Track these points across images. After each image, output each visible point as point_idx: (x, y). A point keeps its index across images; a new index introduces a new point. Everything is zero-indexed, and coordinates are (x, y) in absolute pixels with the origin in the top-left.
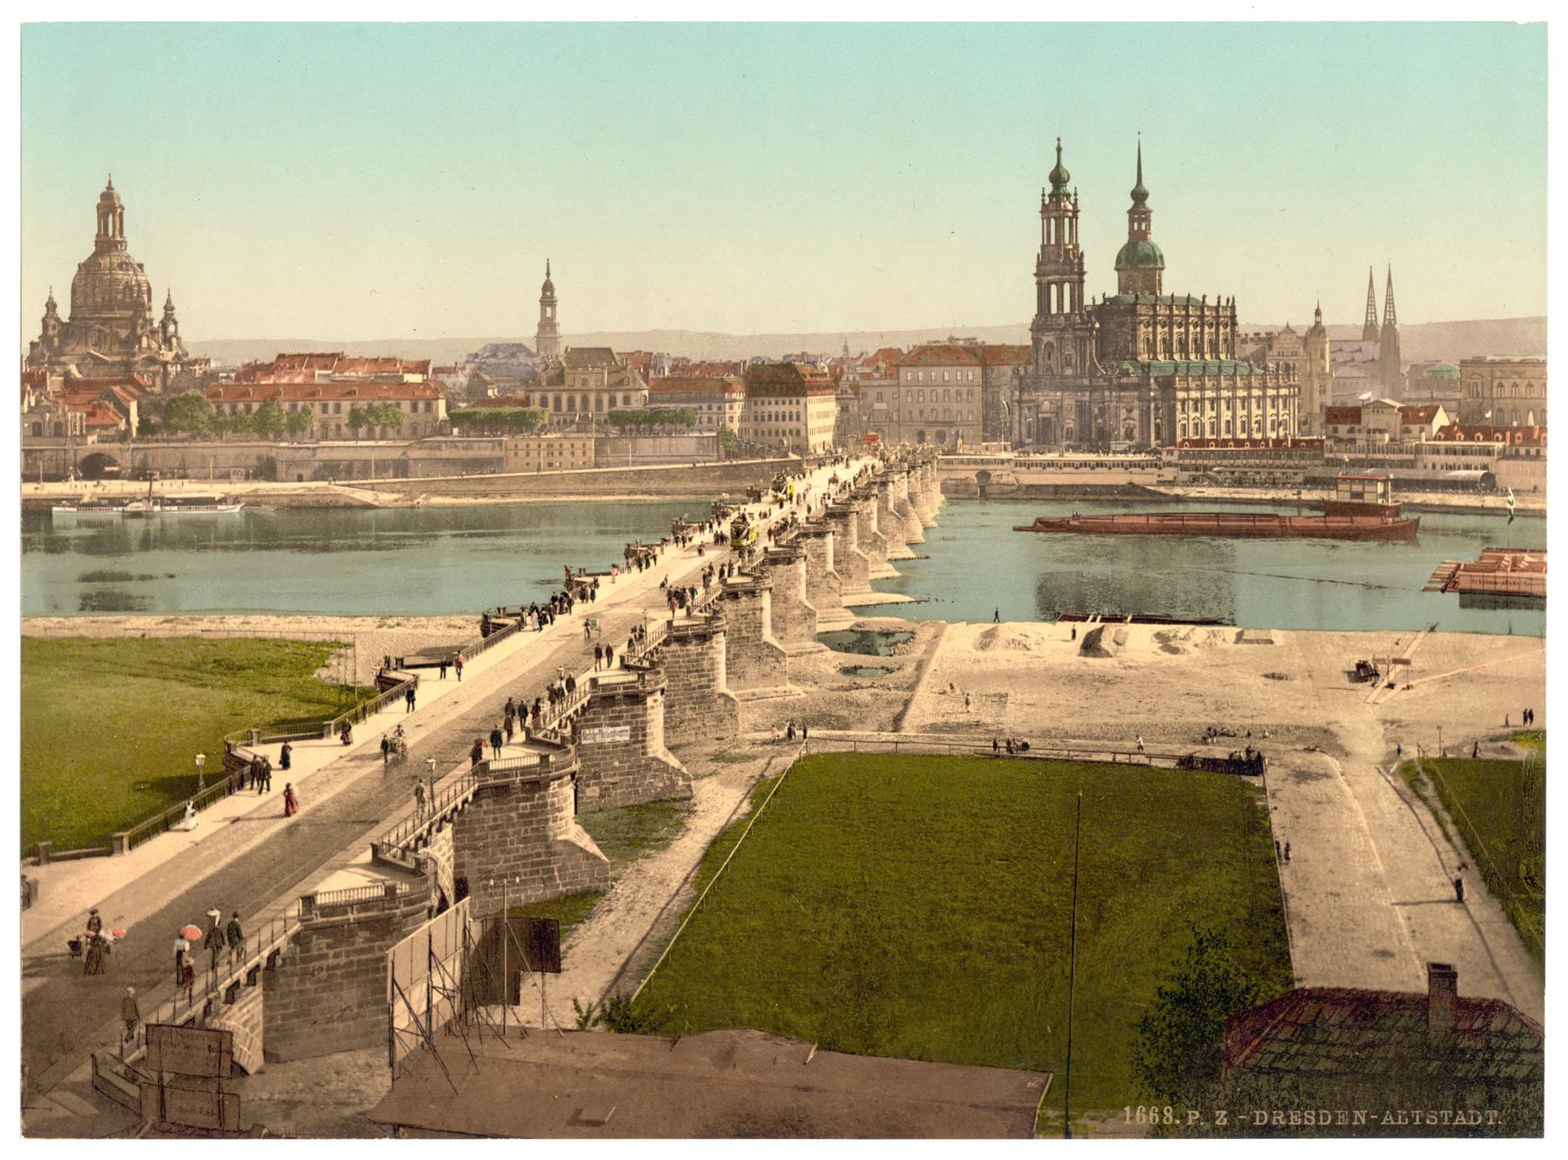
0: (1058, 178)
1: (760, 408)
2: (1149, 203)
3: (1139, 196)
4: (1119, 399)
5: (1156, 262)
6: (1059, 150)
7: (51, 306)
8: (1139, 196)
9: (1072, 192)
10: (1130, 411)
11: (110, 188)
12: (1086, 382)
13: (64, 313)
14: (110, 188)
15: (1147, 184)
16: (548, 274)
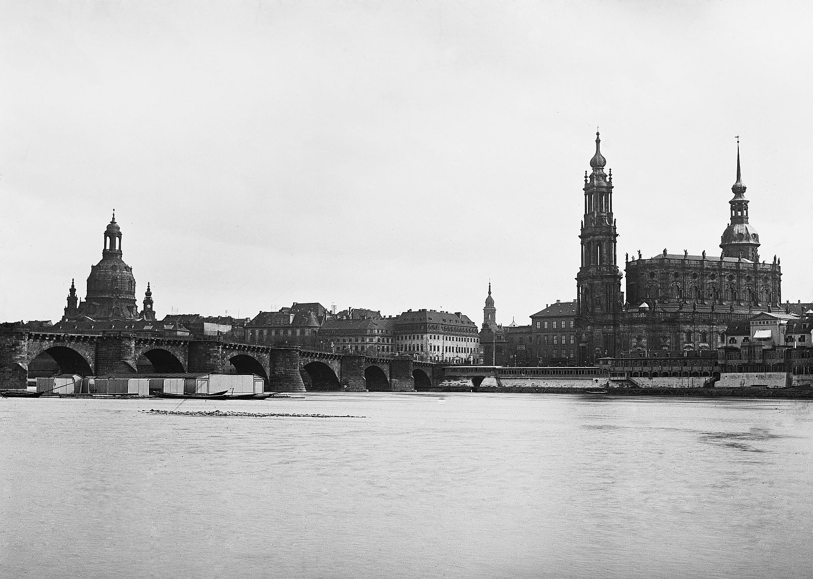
0: (597, 163)
1: (399, 342)
2: (746, 196)
3: (739, 190)
4: (632, 331)
5: (748, 239)
6: (598, 141)
7: (73, 290)
8: (739, 190)
9: (608, 174)
10: (639, 339)
11: (113, 222)
12: (610, 317)
13: (82, 294)
14: (113, 222)
15: (744, 182)
16: (490, 293)
